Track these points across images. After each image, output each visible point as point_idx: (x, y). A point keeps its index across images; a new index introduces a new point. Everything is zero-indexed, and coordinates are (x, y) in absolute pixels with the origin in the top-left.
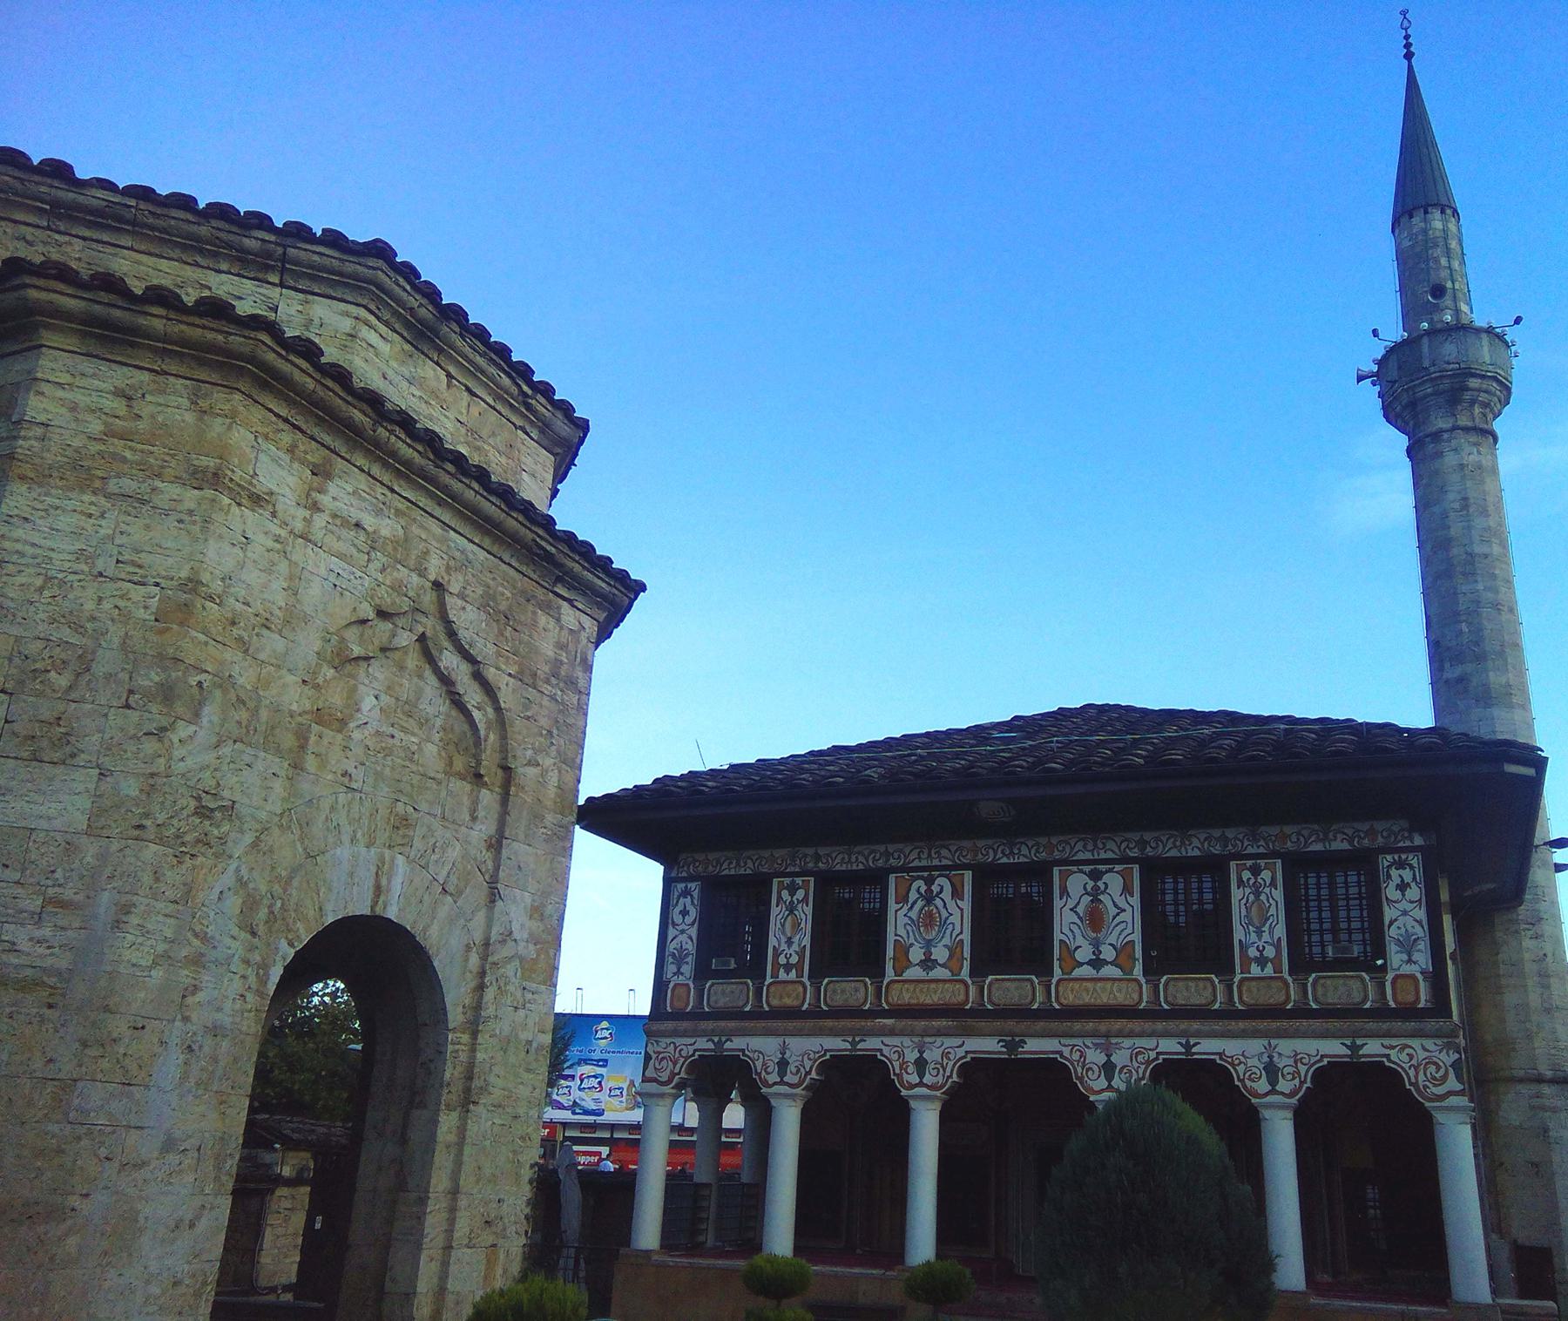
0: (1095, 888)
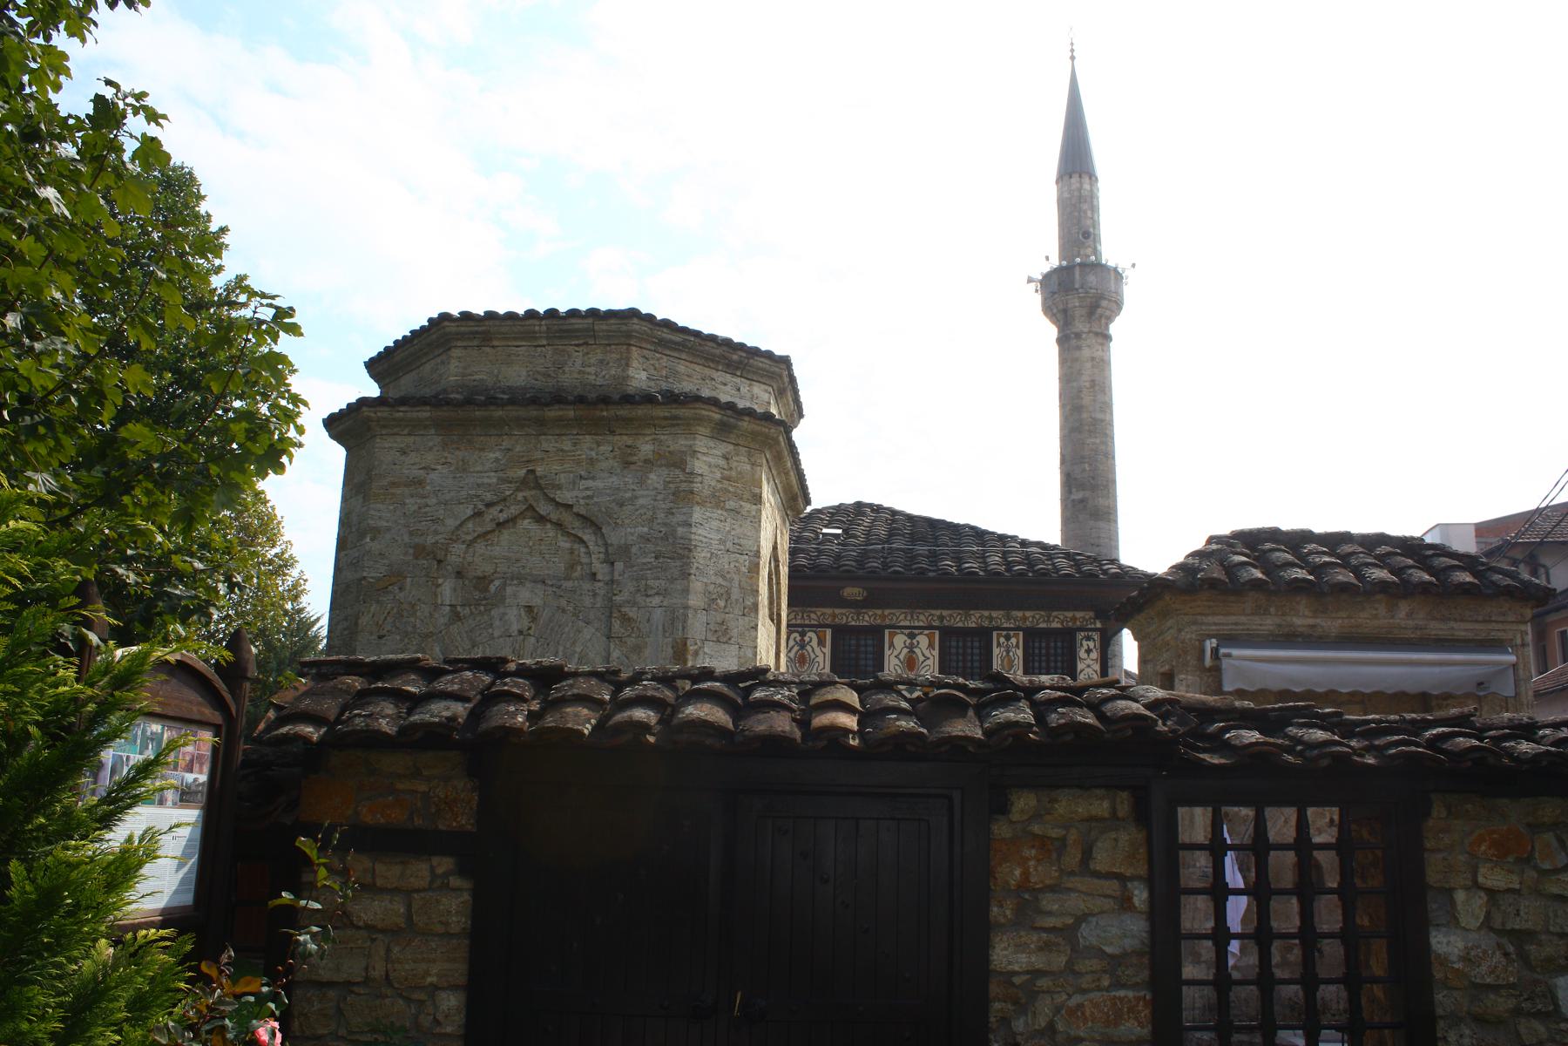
0: (912, 644)
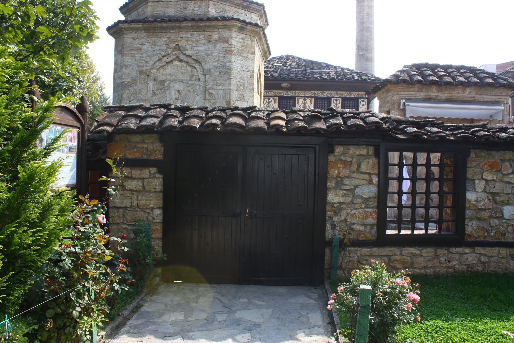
0: (305, 102)
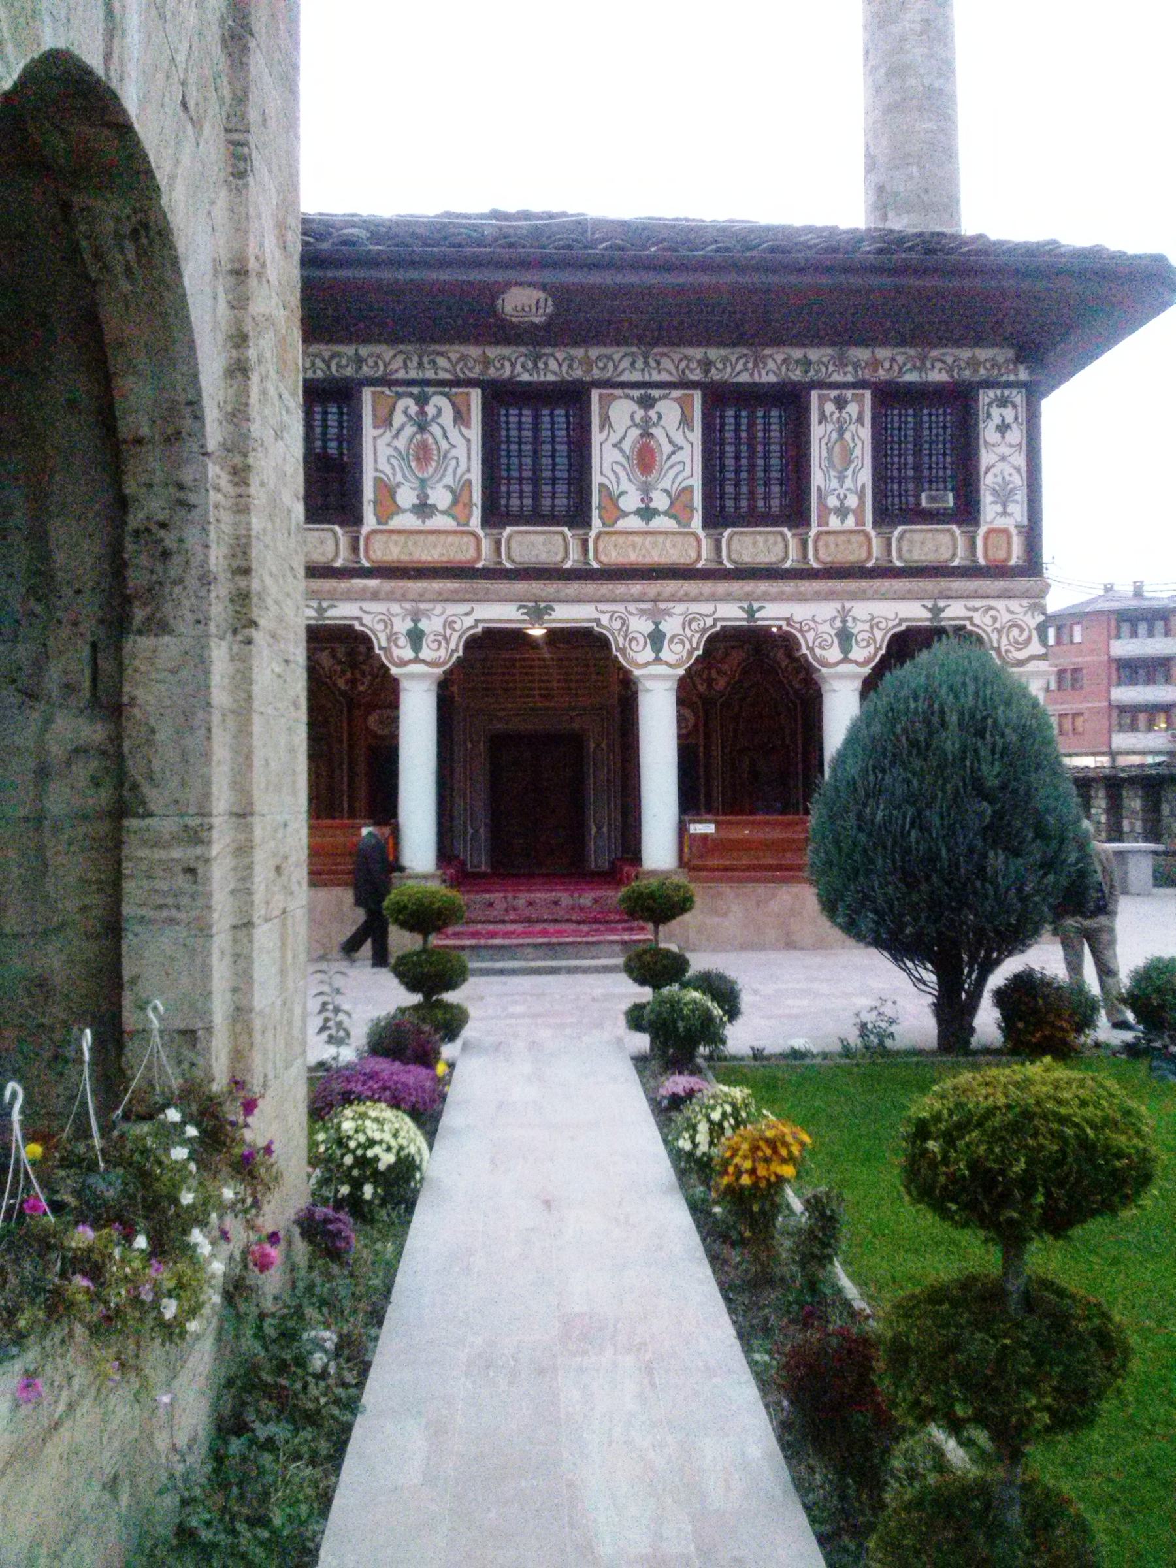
0: (647, 420)
